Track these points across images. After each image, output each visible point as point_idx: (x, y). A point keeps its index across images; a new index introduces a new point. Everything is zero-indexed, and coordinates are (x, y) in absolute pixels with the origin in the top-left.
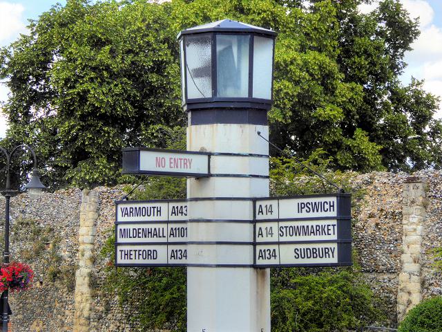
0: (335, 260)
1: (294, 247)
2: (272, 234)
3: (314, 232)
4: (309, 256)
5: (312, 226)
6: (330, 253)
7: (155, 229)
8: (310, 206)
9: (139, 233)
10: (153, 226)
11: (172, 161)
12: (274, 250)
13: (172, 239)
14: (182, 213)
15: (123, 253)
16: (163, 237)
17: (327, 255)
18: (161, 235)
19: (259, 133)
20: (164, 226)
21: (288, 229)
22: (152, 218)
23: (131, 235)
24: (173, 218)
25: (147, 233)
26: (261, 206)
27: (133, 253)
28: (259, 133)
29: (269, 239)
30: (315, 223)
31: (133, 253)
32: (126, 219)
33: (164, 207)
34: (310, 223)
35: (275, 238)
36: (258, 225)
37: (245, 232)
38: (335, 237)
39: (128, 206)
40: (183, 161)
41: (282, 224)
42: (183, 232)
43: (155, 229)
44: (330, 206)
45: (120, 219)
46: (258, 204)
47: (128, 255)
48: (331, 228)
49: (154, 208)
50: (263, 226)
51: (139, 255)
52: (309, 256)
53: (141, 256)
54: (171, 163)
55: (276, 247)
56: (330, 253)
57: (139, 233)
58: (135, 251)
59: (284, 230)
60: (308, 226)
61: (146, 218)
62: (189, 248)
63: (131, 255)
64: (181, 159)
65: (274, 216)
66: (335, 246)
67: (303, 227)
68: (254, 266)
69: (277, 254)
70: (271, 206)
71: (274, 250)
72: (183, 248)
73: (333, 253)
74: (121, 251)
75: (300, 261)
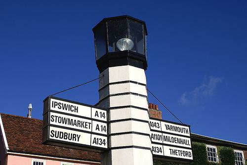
3: (76, 124)
4: (61, 137)
5: (75, 120)
6: (77, 138)
17: (74, 139)
21: (57, 118)
48: (88, 124)
52: (61, 137)
56: (77, 138)
59: (55, 118)
60: (72, 120)
67: (69, 119)
73: (78, 138)
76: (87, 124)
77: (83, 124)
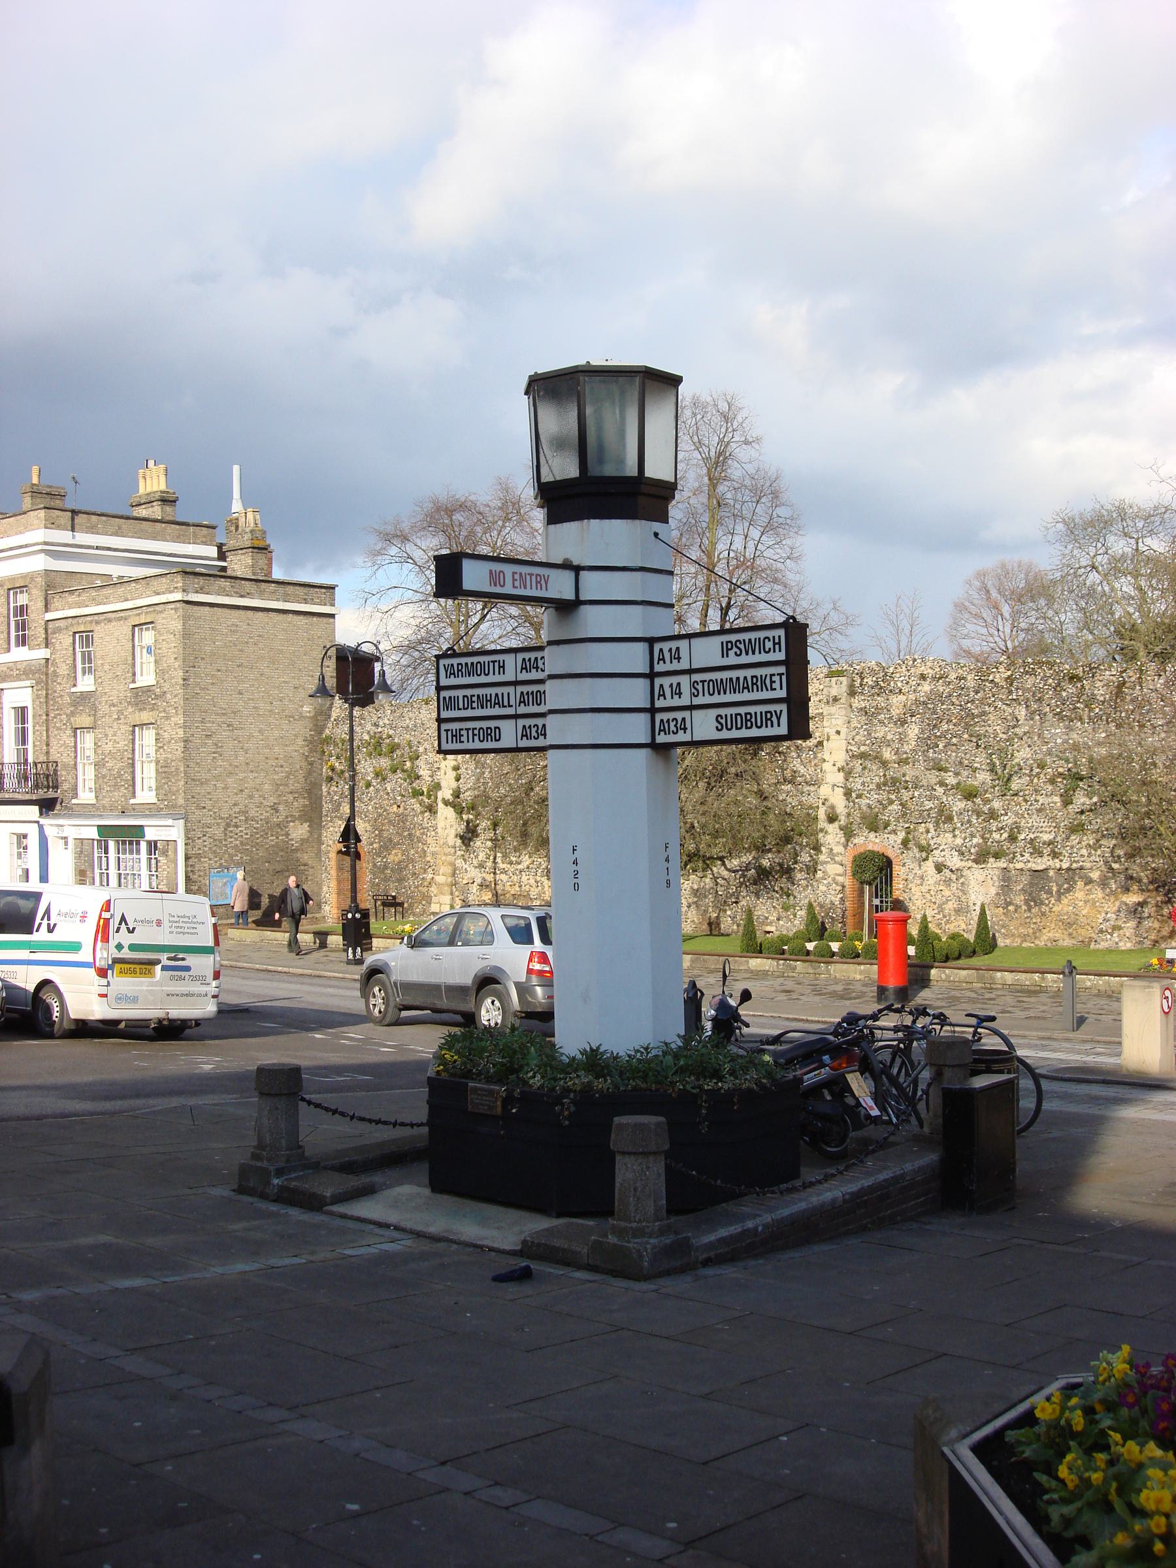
0: (783, 730)
1: (714, 713)
2: (680, 694)
3: (748, 688)
5: (745, 678)
6: (774, 719)
7: (497, 695)
8: (742, 646)
11: (517, 577)
12: (684, 719)
13: (522, 710)
14: (537, 668)
16: (510, 706)
18: (506, 703)
19: (656, 535)
20: (511, 689)
22: (491, 679)
23: (461, 706)
24: (524, 676)
25: (483, 702)
26: (661, 650)
27: (464, 733)
28: (656, 535)
29: (677, 702)
30: (749, 673)
31: (464, 733)
32: (453, 681)
34: (741, 674)
35: (685, 700)
36: (658, 681)
37: (635, 693)
38: (783, 694)
39: (455, 661)
40: (534, 578)
41: (697, 677)
42: (539, 698)
43: (497, 695)
44: (774, 644)
45: (444, 682)
46: (657, 647)
48: (776, 678)
49: (494, 662)
50: (666, 681)
51: (474, 735)
53: (476, 738)
54: (514, 580)
55: (686, 714)
56: (774, 719)
58: (468, 730)
59: (700, 687)
60: (738, 679)
62: (550, 721)
63: (461, 736)
64: (531, 575)
66: (783, 707)
67: (731, 679)
68: (653, 746)
71: (684, 719)
72: (540, 722)
73: (779, 719)
74: (447, 731)
76: (774, 678)
77: (763, 682)
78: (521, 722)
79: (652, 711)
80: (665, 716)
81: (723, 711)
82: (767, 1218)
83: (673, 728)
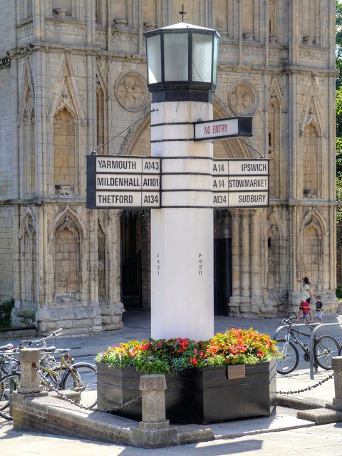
2: (224, 186)
9: (116, 182)
10: (129, 177)
13: (145, 187)
15: (102, 198)
18: (136, 184)
20: (139, 177)
23: (109, 183)
24: (146, 171)
27: (111, 198)
29: (222, 189)
30: (253, 178)
33: (138, 162)
34: (250, 178)
35: (226, 188)
39: (106, 159)
41: (231, 178)
47: (106, 199)
49: (130, 162)
50: (218, 179)
53: (118, 201)
55: (226, 194)
57: (116, 182)
58: (113, 196)
59: (232, 183)
61: (123, 170)
65: (225, 172)
66: (266, 193)
69: (227, 198)
70: (223, 165)
74: (100, 196)
75: (242, 204)
78: (145, 194)
79: (161, 191)
80: (217, 195)
81: (242, 194)
82: (163, 430)
83: (220, 200)
